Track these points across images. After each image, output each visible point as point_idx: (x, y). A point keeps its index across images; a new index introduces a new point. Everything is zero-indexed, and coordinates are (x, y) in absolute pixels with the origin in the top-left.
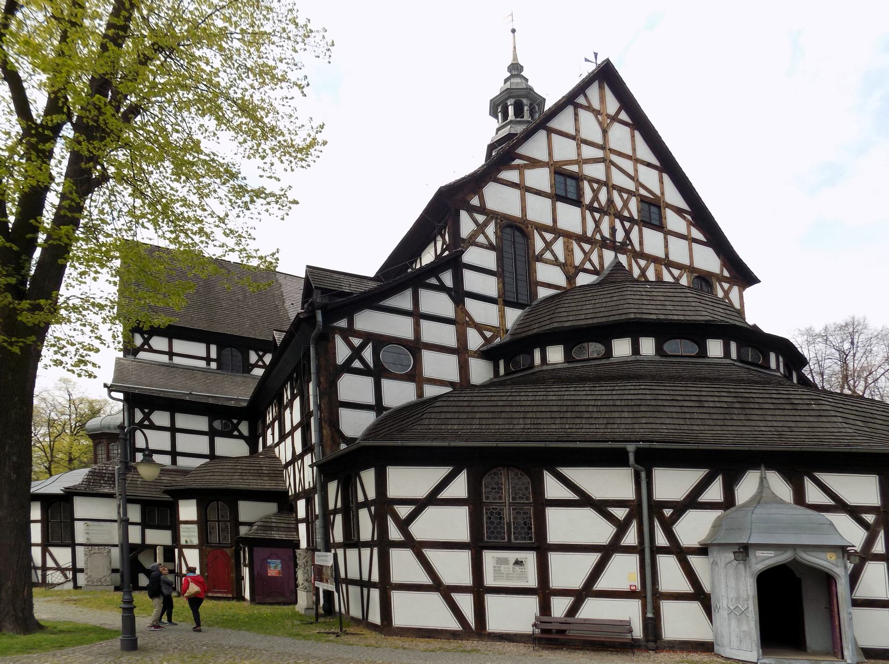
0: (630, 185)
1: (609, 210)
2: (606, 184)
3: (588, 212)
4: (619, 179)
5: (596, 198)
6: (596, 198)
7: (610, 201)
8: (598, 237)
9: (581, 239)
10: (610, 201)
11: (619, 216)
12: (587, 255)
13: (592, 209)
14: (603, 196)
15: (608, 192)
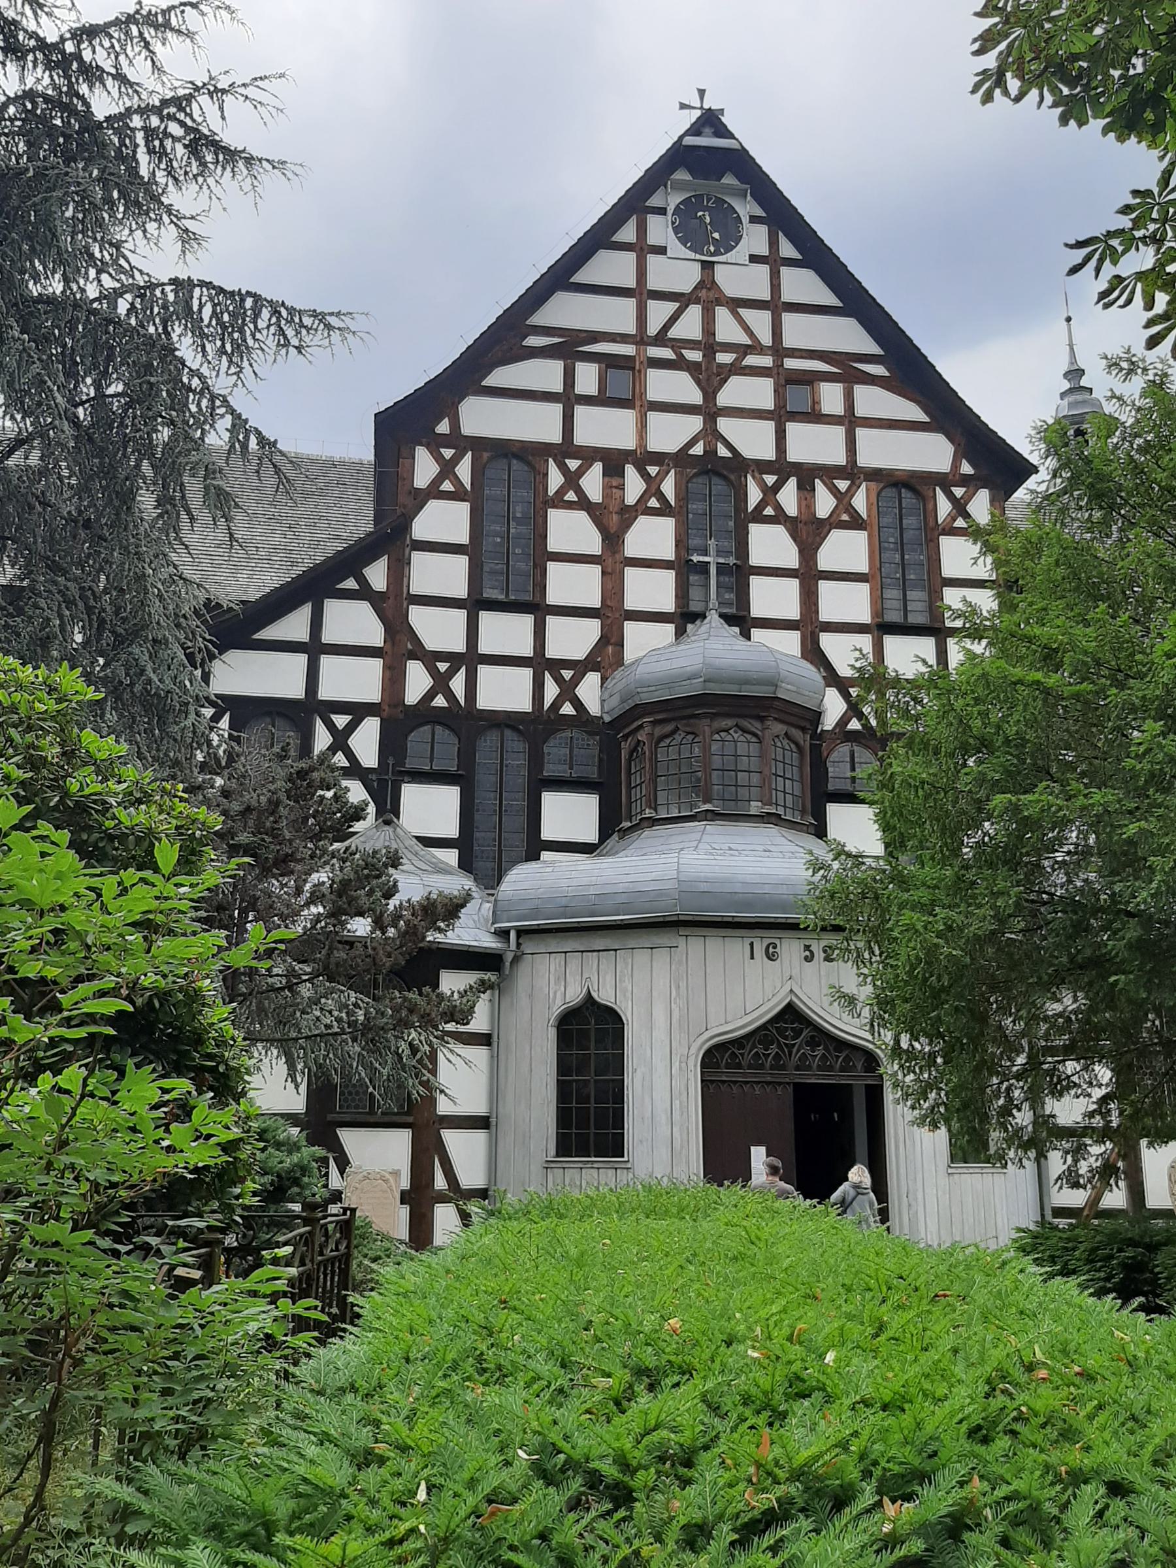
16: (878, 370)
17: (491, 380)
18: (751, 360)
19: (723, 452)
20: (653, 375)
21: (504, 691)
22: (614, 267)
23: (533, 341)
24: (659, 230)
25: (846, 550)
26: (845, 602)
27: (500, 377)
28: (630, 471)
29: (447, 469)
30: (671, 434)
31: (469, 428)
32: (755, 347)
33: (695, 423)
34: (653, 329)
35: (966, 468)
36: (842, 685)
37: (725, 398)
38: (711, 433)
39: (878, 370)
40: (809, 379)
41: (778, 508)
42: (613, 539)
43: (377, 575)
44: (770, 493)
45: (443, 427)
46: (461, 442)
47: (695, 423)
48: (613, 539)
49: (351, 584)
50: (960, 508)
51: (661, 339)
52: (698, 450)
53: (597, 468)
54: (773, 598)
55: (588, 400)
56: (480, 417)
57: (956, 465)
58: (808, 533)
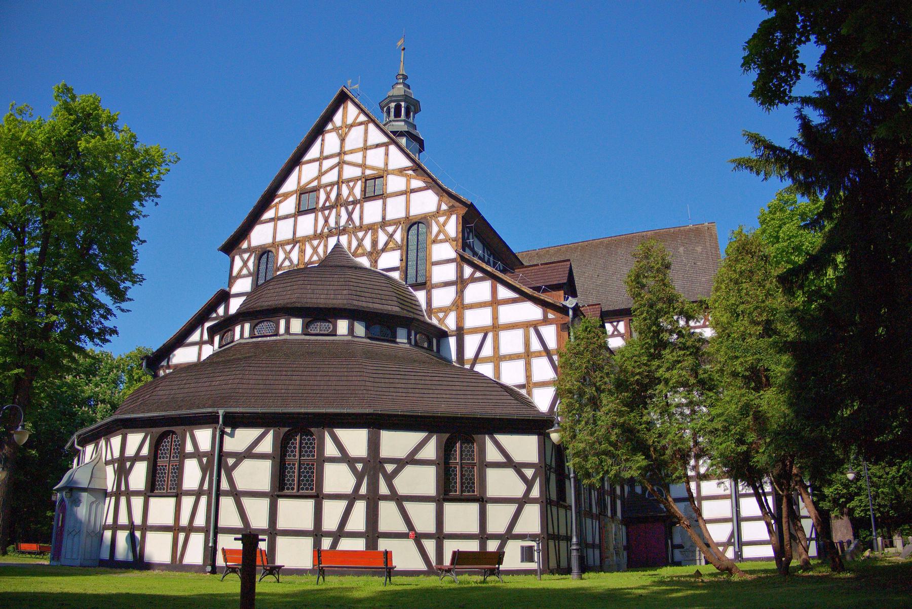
0: (357, 172)
1: (339, 203)
2: (337, 183)
3: (320, 214)
4: (350, 172)
5: (328, 198)
6: (328, 198)
7: (339, 195)
8: (326, 230)
9: (316, 236)
10: (339, 195)
11: (346, 204)
12: (315, 250)
13: (324, 208)
14: (333, 196)
15: (338, 188)
29: (245, 263)
45: (245, 245)
46: (250, 250)
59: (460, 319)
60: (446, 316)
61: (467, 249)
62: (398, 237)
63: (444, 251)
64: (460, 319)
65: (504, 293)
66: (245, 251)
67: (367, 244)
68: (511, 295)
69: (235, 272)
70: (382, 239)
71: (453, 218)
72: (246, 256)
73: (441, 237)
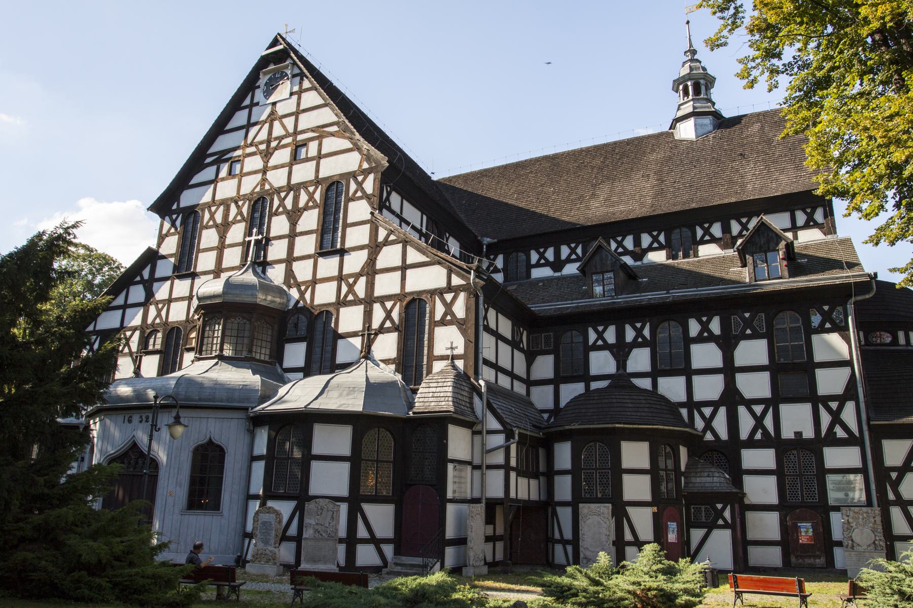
16: (334, 129)
17: (193, 182)
18: (284, 142)
19: (267, 187)
20: (247, 160)
21: (178, 313)
22: (240, 118)
23: (209, 160)
24: (259, 95)
25: (310, 220)
26: (306, 245)
27: (196, 179)
28: (233, 206)
30: (249, 185)
31: (182, 205)
32: (287, 135)
33: (259, 177)
34: (249, 141)
35: (366, 166)
36: (298, 285)
37: (272, 163)
38: (264, 180)
39: (334, 129)
40: (304, 144)
41: (284, 207)
42: (222, 237)
43: (146, 274)
44: (282, 200)
45: (175, 207)
46: (179, 211)
47: (259, 177)
48: (222, 237)
49: (138, 278)
50: (360, 185)
51: (251, 145)
52: (258, 189)
53: (222, 208)
54: (278, 250)
55: (223, 179)
56: (187, 199)
57: (360, 166)
58: (294, 216)
59: (370, 286)
60: (355, 282)
61: (384, 211)
62: (317, 196)
63: (359, 210)
64: (370, 286)
65: (414, 256)
66: (174, 212)
67: (289, 203)
68: (420, 258)
69: (164, 232)
70: (303, 198)
71: (371, 177)
72: (174, 217)
73: (359, 194)
